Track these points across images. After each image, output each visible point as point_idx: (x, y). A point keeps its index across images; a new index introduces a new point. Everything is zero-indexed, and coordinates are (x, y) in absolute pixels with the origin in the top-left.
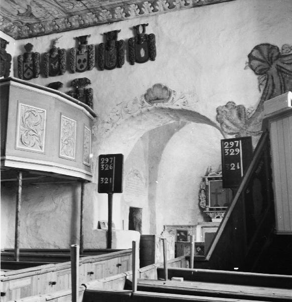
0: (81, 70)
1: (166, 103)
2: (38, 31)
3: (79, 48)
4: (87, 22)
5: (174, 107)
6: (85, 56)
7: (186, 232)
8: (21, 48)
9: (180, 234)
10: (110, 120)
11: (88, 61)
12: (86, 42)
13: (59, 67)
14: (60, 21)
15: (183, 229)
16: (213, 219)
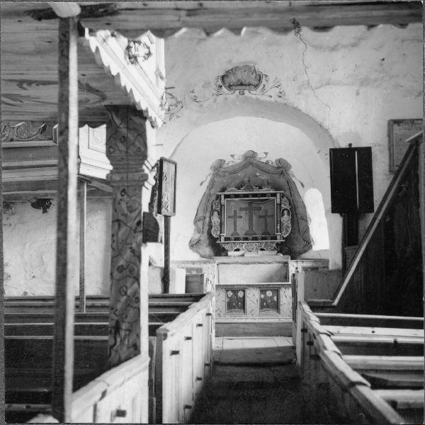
1: (254, 92)
5: (265, 98)
15: (196, 266)
16: (229, 253)
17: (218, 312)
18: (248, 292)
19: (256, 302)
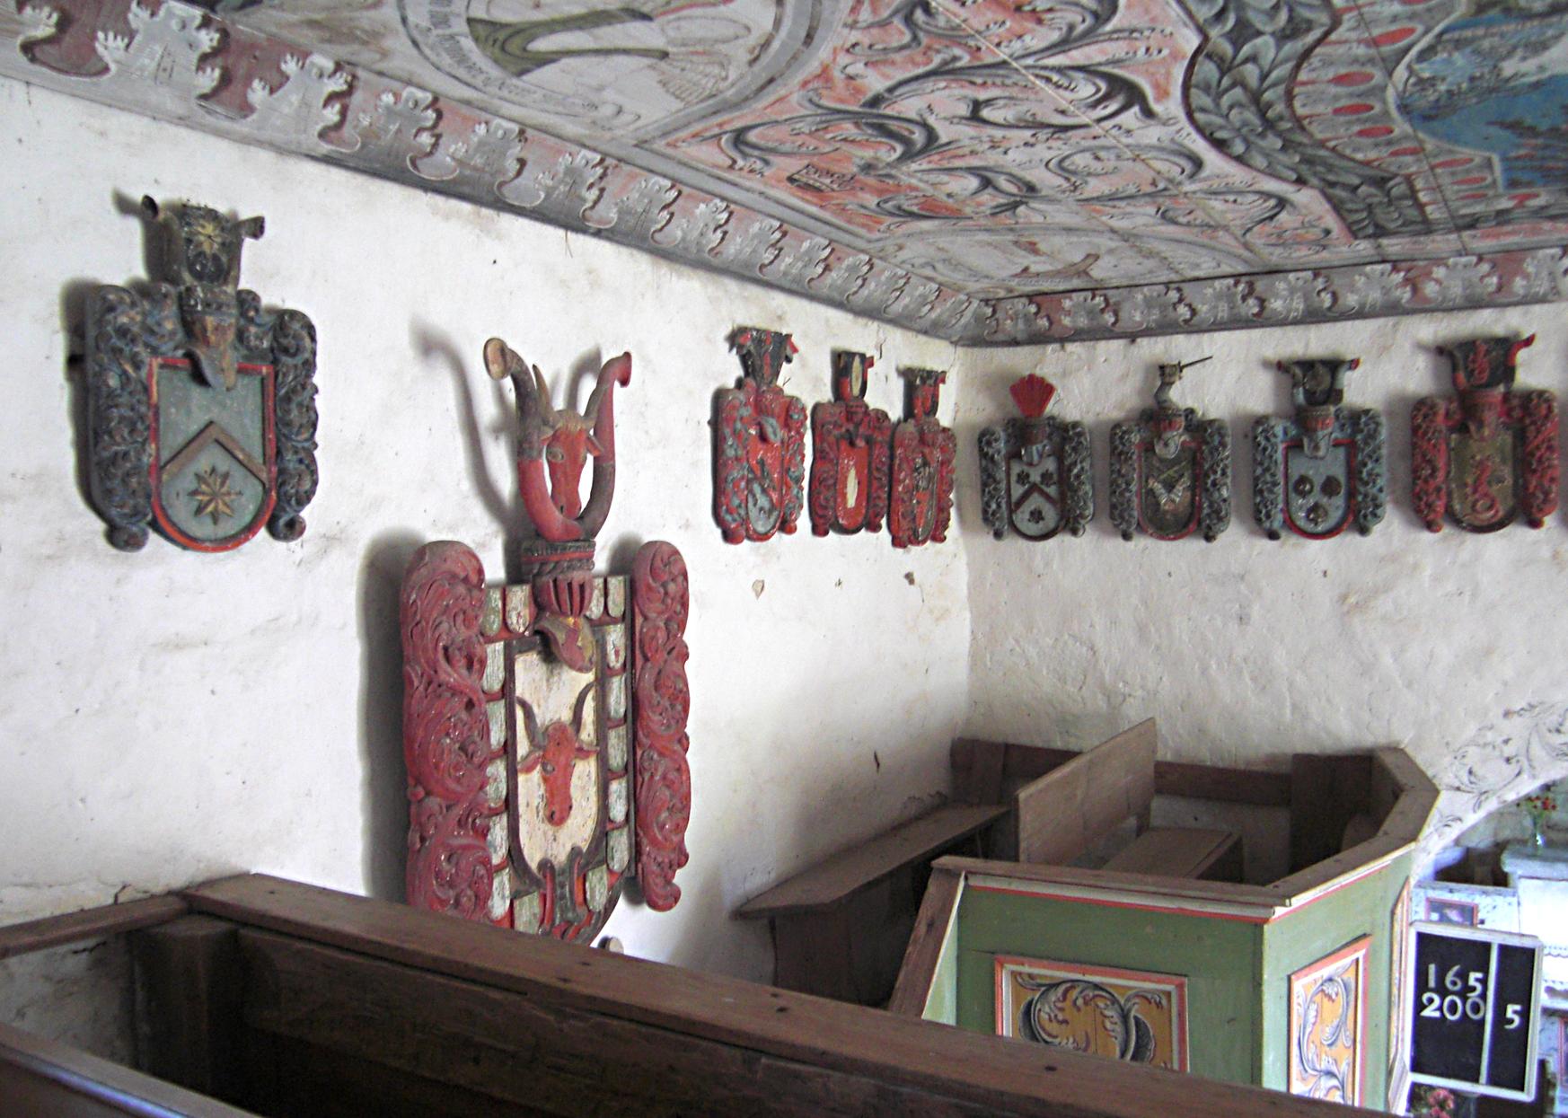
0: (1310, 527)
2: (1083, 322)
3: (1303, 420)
4: (1351, 300)
6: (1332, 464)
8: (989, 383)
10: (1465, 778)
11: (1351, 494)
12: (1335, 395)
13: (1194, 507)
14: (1210, 291)
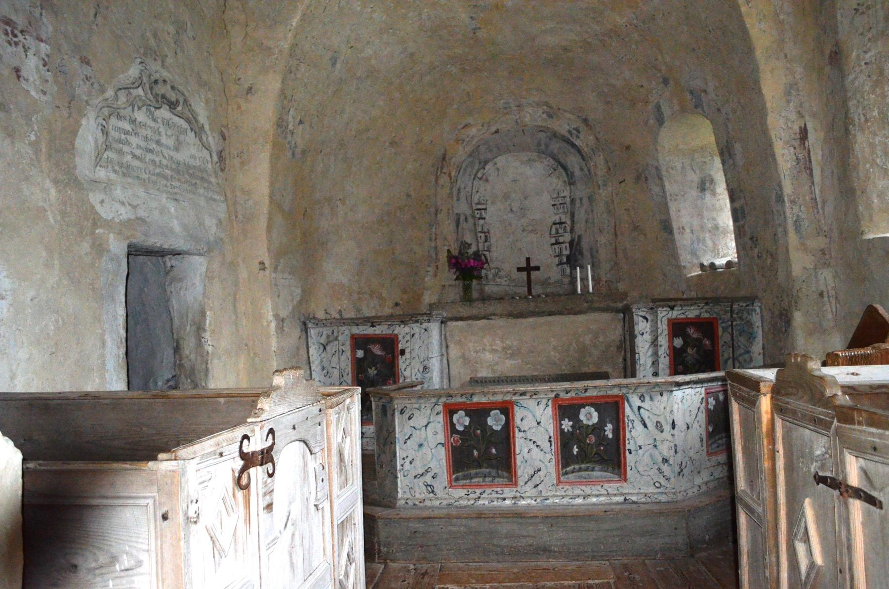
7: (390, 344)
9: (367, 352)
15: (378, 330)
17: (428, 478)
18: (518, 413)
19: (546, 445)
